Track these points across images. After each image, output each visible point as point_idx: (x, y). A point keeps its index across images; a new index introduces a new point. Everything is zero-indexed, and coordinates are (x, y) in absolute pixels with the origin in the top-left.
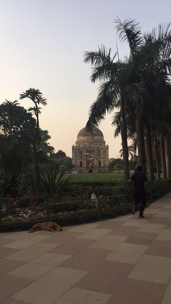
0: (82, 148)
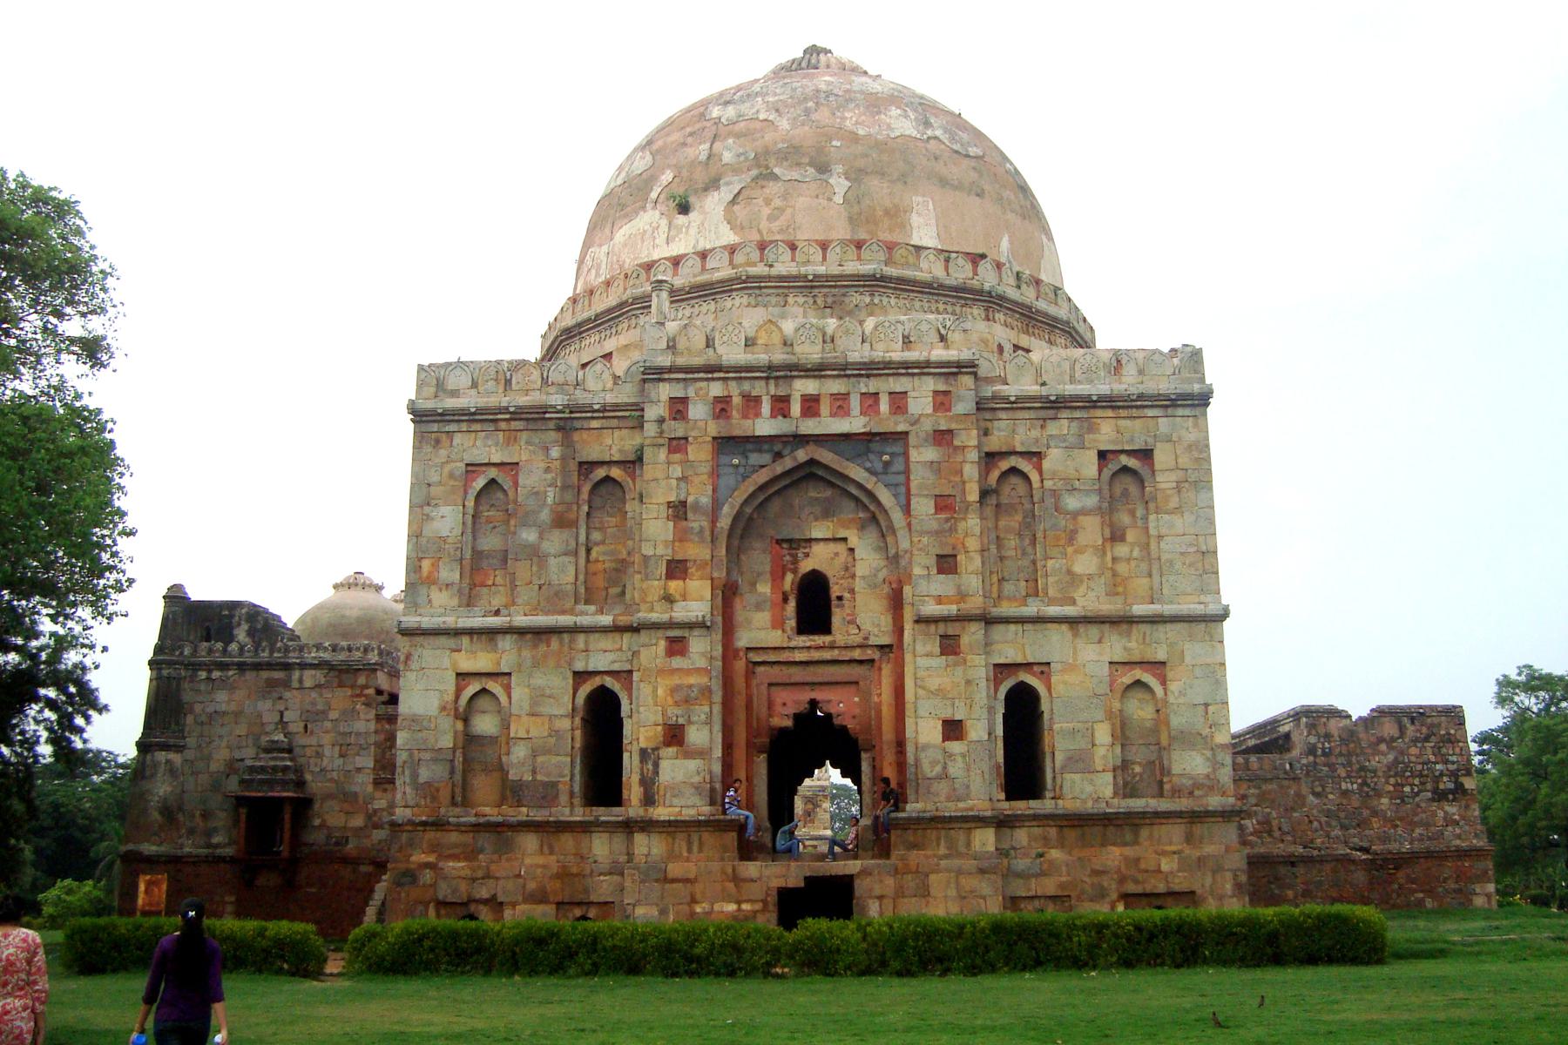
0: (625, 395)
